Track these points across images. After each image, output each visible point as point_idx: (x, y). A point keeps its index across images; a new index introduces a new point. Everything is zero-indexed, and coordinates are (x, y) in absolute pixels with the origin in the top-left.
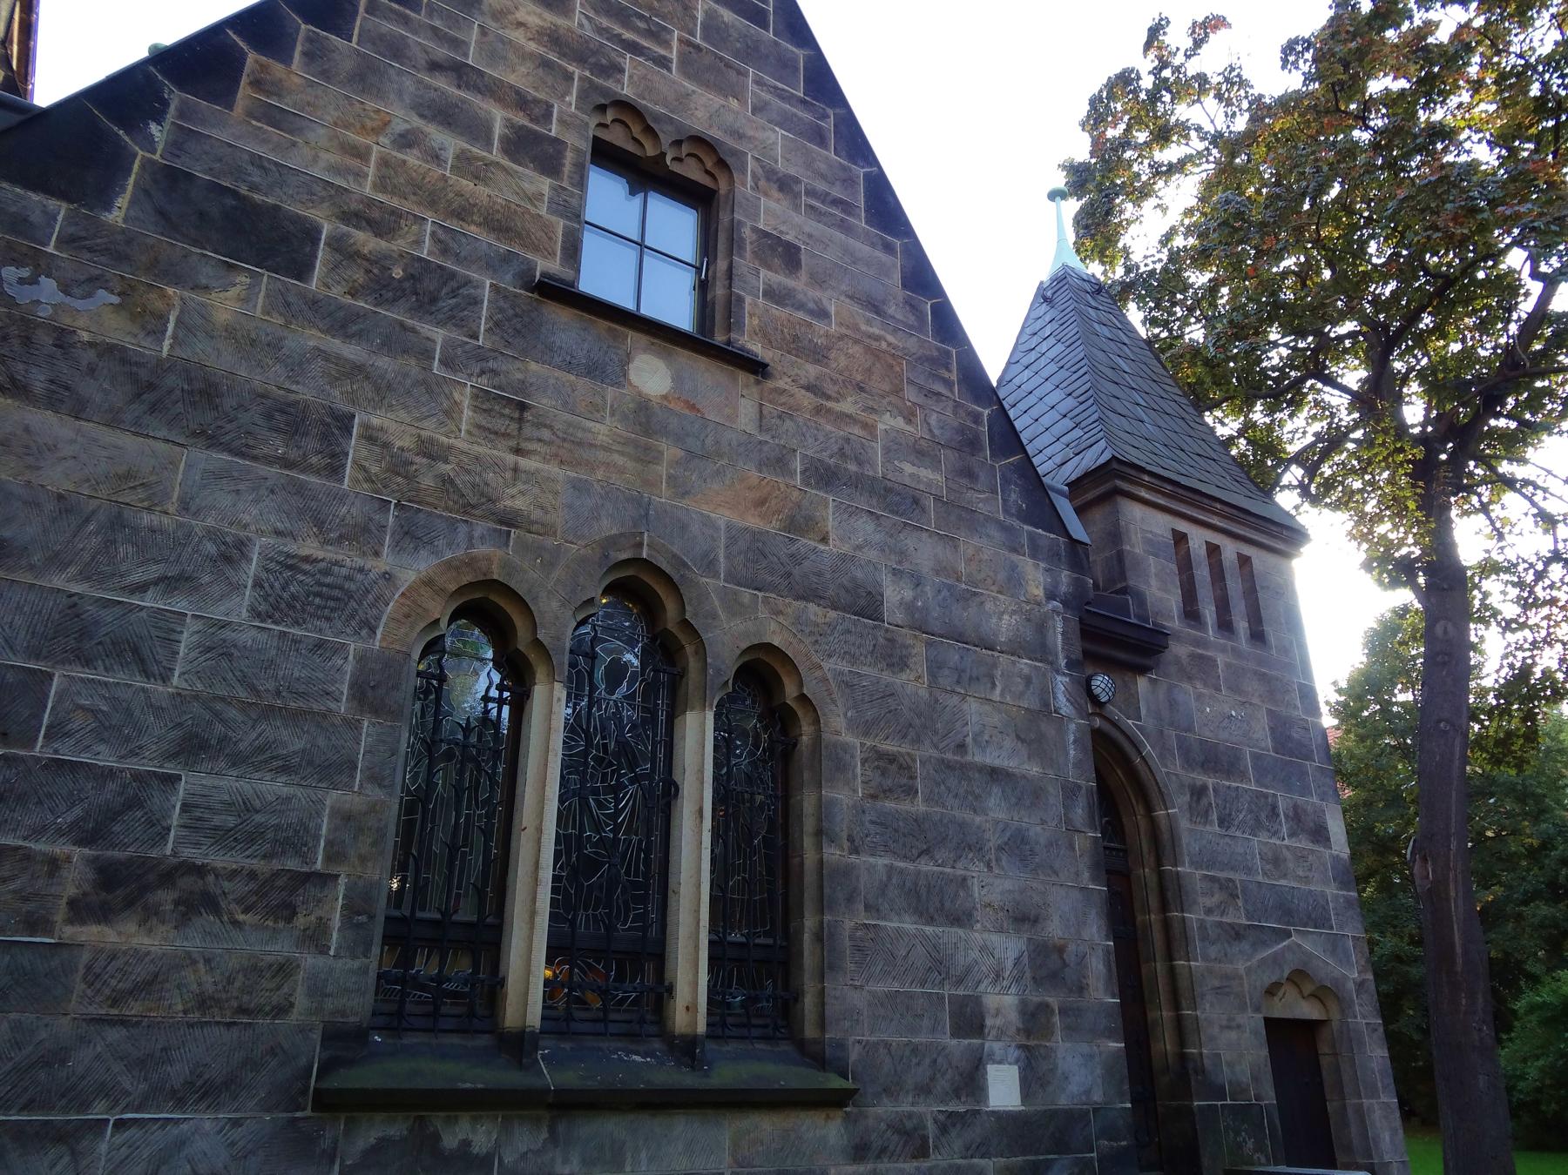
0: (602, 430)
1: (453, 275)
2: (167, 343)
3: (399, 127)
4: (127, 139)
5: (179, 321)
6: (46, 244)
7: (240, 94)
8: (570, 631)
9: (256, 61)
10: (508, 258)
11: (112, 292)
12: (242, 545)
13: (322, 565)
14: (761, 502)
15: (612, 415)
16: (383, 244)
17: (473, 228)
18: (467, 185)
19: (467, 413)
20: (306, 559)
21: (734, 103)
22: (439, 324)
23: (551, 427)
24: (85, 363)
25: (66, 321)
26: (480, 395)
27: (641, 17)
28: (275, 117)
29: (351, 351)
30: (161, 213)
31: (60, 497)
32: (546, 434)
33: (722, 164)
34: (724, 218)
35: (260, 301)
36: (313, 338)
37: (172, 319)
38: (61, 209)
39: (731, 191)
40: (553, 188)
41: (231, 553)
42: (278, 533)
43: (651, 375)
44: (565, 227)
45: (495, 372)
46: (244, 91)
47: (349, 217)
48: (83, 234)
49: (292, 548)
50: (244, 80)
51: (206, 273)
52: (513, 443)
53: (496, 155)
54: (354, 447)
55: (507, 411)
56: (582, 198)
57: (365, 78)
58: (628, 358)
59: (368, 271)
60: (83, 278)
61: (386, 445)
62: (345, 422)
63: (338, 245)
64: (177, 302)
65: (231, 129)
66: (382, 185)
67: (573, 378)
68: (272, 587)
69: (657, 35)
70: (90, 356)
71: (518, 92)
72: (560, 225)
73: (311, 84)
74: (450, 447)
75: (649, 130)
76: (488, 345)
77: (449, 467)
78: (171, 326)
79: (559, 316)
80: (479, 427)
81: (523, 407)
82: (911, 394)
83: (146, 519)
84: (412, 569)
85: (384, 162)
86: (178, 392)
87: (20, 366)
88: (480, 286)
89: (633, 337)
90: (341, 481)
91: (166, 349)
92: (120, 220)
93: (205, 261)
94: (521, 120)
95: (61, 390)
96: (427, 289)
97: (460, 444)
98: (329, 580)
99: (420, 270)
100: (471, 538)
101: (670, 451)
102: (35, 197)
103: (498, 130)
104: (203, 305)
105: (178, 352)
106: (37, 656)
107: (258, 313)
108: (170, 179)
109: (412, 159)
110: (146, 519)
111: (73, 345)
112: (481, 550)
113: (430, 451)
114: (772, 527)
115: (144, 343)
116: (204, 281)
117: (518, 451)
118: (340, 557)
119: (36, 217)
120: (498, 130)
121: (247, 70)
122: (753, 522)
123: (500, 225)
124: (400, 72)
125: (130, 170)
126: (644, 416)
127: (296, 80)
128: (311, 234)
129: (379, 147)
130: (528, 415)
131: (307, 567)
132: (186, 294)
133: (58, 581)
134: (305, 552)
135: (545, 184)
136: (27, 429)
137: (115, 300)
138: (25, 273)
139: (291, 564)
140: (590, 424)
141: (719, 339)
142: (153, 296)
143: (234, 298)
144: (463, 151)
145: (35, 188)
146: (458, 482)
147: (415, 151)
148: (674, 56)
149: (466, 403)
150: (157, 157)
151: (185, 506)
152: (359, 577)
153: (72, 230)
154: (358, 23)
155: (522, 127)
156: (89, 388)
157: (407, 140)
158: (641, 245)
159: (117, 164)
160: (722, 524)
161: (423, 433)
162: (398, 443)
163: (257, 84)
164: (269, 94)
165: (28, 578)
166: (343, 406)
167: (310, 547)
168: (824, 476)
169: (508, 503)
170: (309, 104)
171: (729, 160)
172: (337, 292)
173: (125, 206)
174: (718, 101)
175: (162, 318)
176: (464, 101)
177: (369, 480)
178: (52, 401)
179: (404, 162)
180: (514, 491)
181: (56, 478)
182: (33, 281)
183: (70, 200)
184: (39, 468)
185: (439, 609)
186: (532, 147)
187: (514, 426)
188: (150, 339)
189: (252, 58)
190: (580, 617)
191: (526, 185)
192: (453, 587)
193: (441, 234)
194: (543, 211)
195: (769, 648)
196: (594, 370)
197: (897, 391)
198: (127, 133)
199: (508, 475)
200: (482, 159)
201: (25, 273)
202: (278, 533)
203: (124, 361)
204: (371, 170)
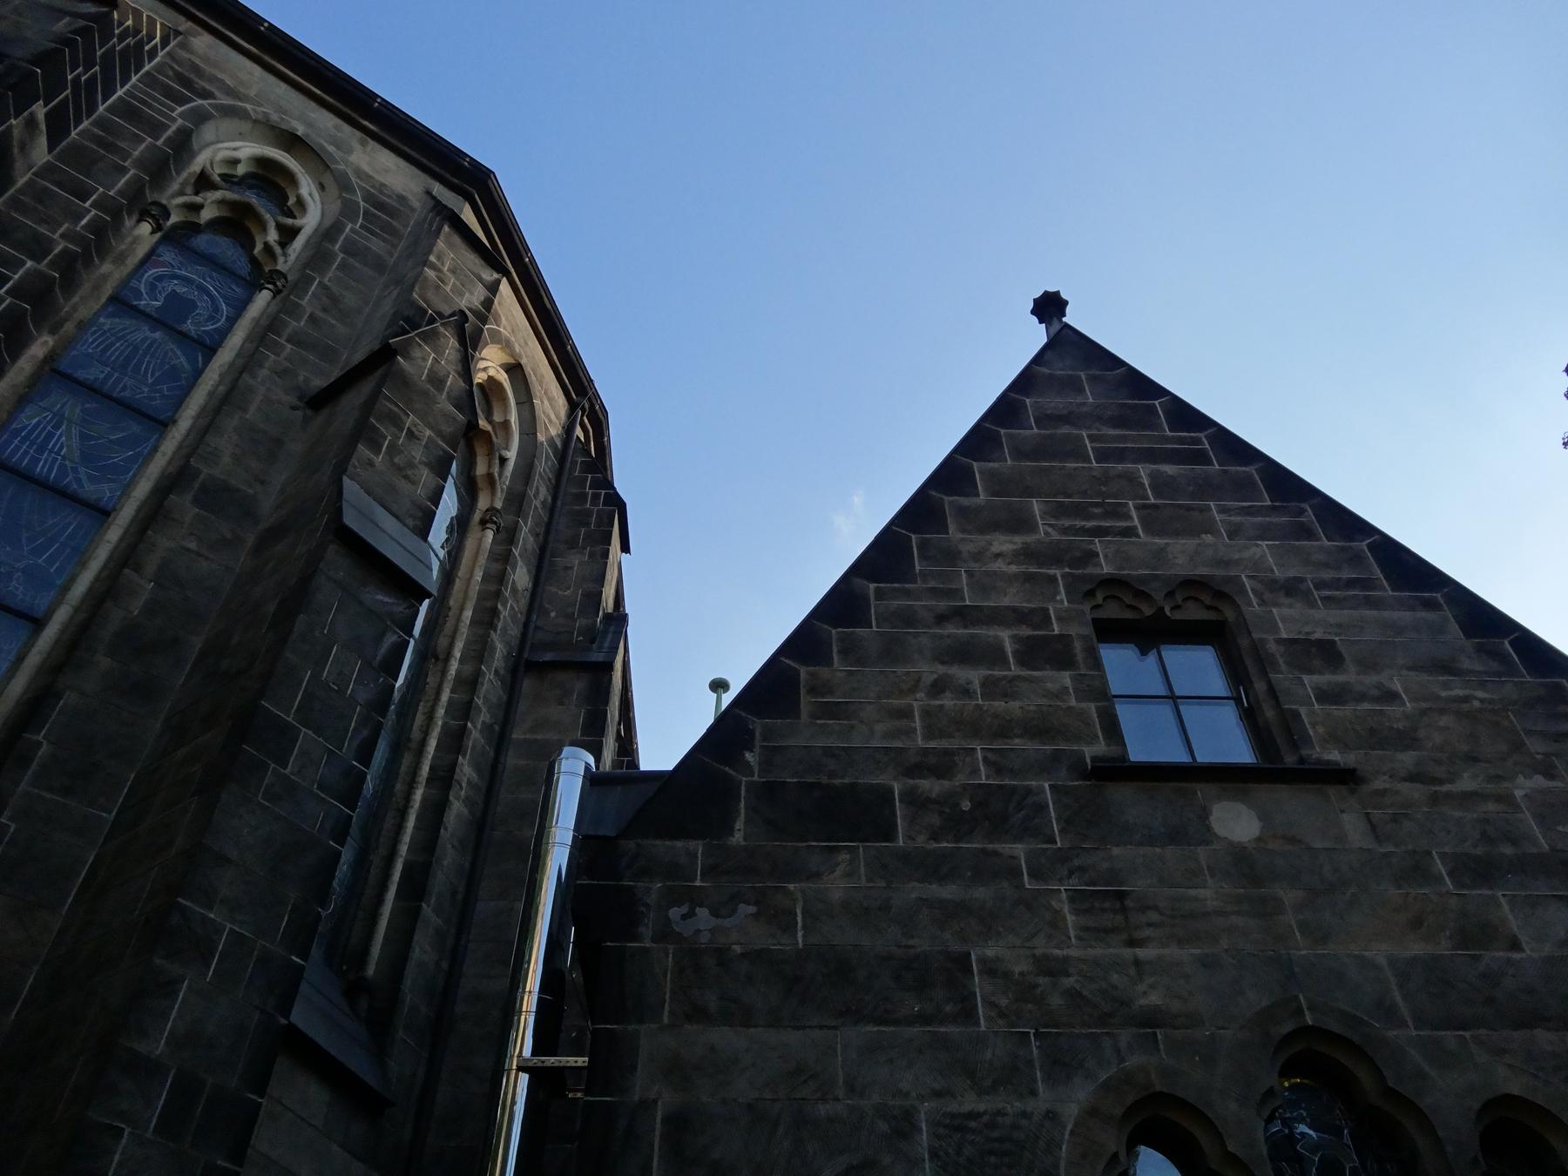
0: (1208, 894)
1: (1014, 789)
2: (800, 934)
3: (928, 679)
8: (1260, 1135)
10: (1056, 756)
12: (909, 1115)
13: (985, 1119)
14: (1417, 923)
15: (1213, 876)
16: (946, 783)
17: (1017, 741)
18: (999, 705)
19: (1070, 918)
20: (972, 1115)
21: (1208, 538)
22: (1017, 839)
23: (1156, 908)
26: (1075, 897)
27: (1096, 505)
28: (832, 711)
29: (949, 892)
32: (1154, 916)
33: (1220, 595)
34: (1244, 642)
35: (862, 870)
36: (914, 890)
38: (698, 846)
39: (1240, 613)
40: (1073, 679)
41: (904, 1126)
42: (938, 1094)
43: (1236, 822)
44: (1097, 708)
45: (1082, 869)
46: (806, 701)
47: (914, 770)
49: (953, 1107)
50: (803, 691)
52: (1124, 936)
53: (1015, 670)
54: (979, 985)
55: (1107, 905)
56: (1103, 677)
57: (892, 651)
58: (1204, 814)
59: (941, 813)
61: (1007, 975)
62: (963, 961)
63: (911, 798)
64: (799, 895)
65: (805, 734)
66: (930, 733)
67: (1158, 850)
68: (947, 1154)
69: (1117, 512)
71: (1014, 610)
72: (1092, 708)
74: (1066, 959)
75: (1142, 595)
76: (1067, 845)
77: (1072, 979)
78: (799, 919)
79: (1121, 794)
80: (1088, 929)
81: (1121, 896)
82: (1536, 746)
83: (823, 1110)
84: (1074, 1100)
85: (927, 713)
88: (1042, 790)
89: (1201, 790)
90: (978, 1024)
94: (1026, 631)
96: (998, 811)
97: (1073, 953)
98: (996, 1134)
99: (983, 796)
100: (1118, 1051)
101: (1289, 896)
102: (679, 844)
103: (1009, 648)
107: (863, 882)
108: (769, 791)
109: (948, 701)
110: (823, 1110)
112: (1134, 1061)
113: (1052, 968)
114: (1444, 948)
117: (1132, 943)
118: (1001, 1105)
120: (1009, 648)
122: (1417, 948)
123: (1039, 728)
124: (916, 635)
126: (1242, 863)
127: (839, 674)
128: (885, 795)
129: (918, 701)
130: (1129, 903)
131: (973, 1124)
134: (967, 1108)
135: (1066, 678)
137: (752, 909)
138: (684, 909)
139: (957, 1125)
140: (1193, 892)
141: (1290, 760)
143: (842, 876)
144: (987, 678)
146: (1085, 993)
147: (948, 694)
148: (1136, 522)
149: (1066, 909)
150: (756, 778)
151: (851, 1088)
152: (1024, 1122)
155: (1029, 637)
157: (938, 688)
158: (1173, 698)
160: (1382, 961)
161: (1038, 952)
162: (1017, 969)
163: (812, 690)
166: (956, 947)
167: (969, 1102)
168: (1478, 870)
169: (1143, 1002)
171: (1226, 589)
172: (921, 840)
174: (1190, 543)
176: (972, 636)
177: (1002, 1015)
179: (942, 706)
180: (1141, 988)
182: (690, 915)
185: (1112, 1141)
186: (1044, 652)
187: (1119, 918)
189: (804, 672)
190: (1266, 1114)
191: (1049, 685)
192: (1119, 1111)
193: (990, 755)
194: (1073, 703)
195: (1508, 1100)
196: (1176, 836)
197: (1518, 746)
199: (1132, 971)
200: (1005, 677)
201: (684, 909)
202: (938, 1094)
204: (918, 723)
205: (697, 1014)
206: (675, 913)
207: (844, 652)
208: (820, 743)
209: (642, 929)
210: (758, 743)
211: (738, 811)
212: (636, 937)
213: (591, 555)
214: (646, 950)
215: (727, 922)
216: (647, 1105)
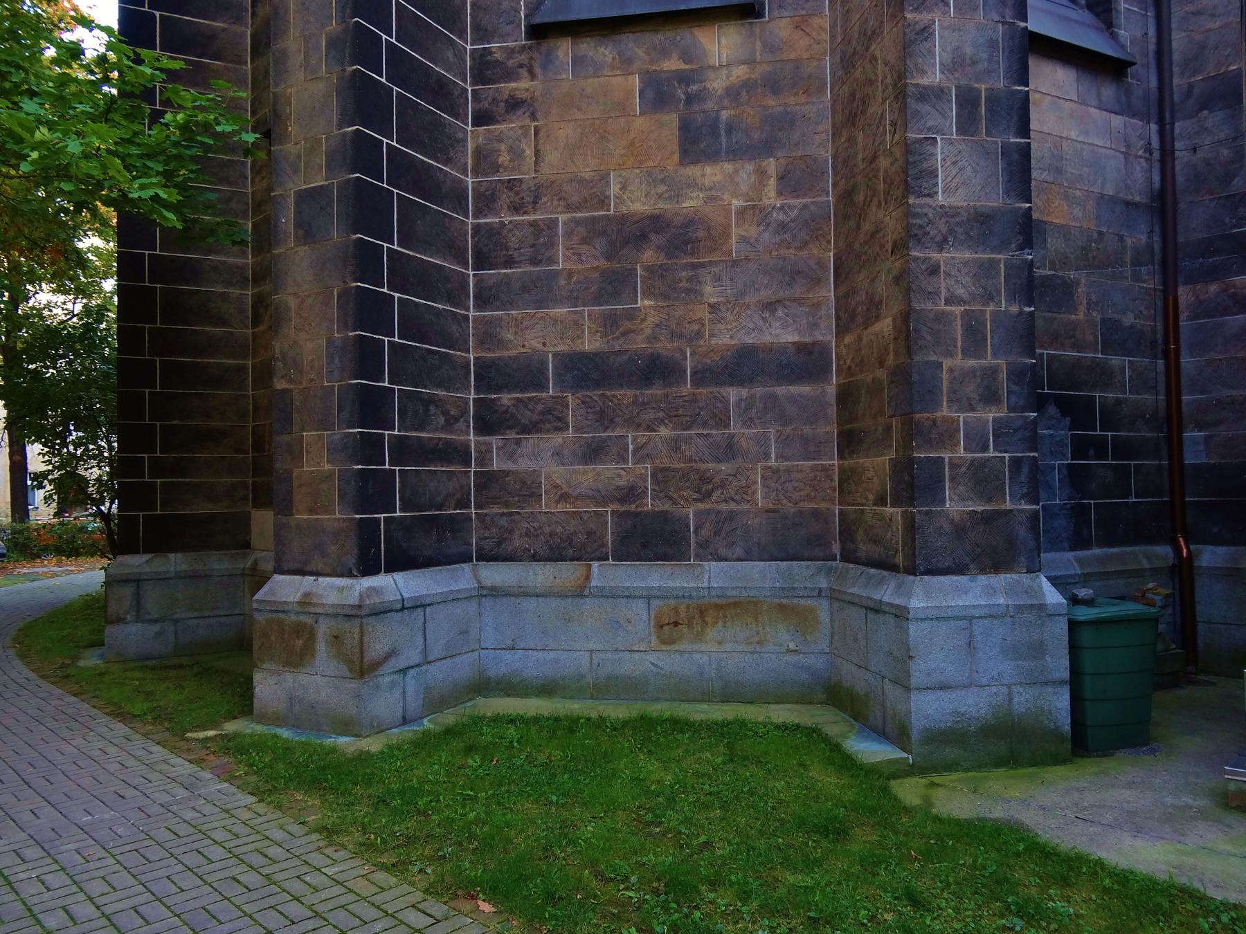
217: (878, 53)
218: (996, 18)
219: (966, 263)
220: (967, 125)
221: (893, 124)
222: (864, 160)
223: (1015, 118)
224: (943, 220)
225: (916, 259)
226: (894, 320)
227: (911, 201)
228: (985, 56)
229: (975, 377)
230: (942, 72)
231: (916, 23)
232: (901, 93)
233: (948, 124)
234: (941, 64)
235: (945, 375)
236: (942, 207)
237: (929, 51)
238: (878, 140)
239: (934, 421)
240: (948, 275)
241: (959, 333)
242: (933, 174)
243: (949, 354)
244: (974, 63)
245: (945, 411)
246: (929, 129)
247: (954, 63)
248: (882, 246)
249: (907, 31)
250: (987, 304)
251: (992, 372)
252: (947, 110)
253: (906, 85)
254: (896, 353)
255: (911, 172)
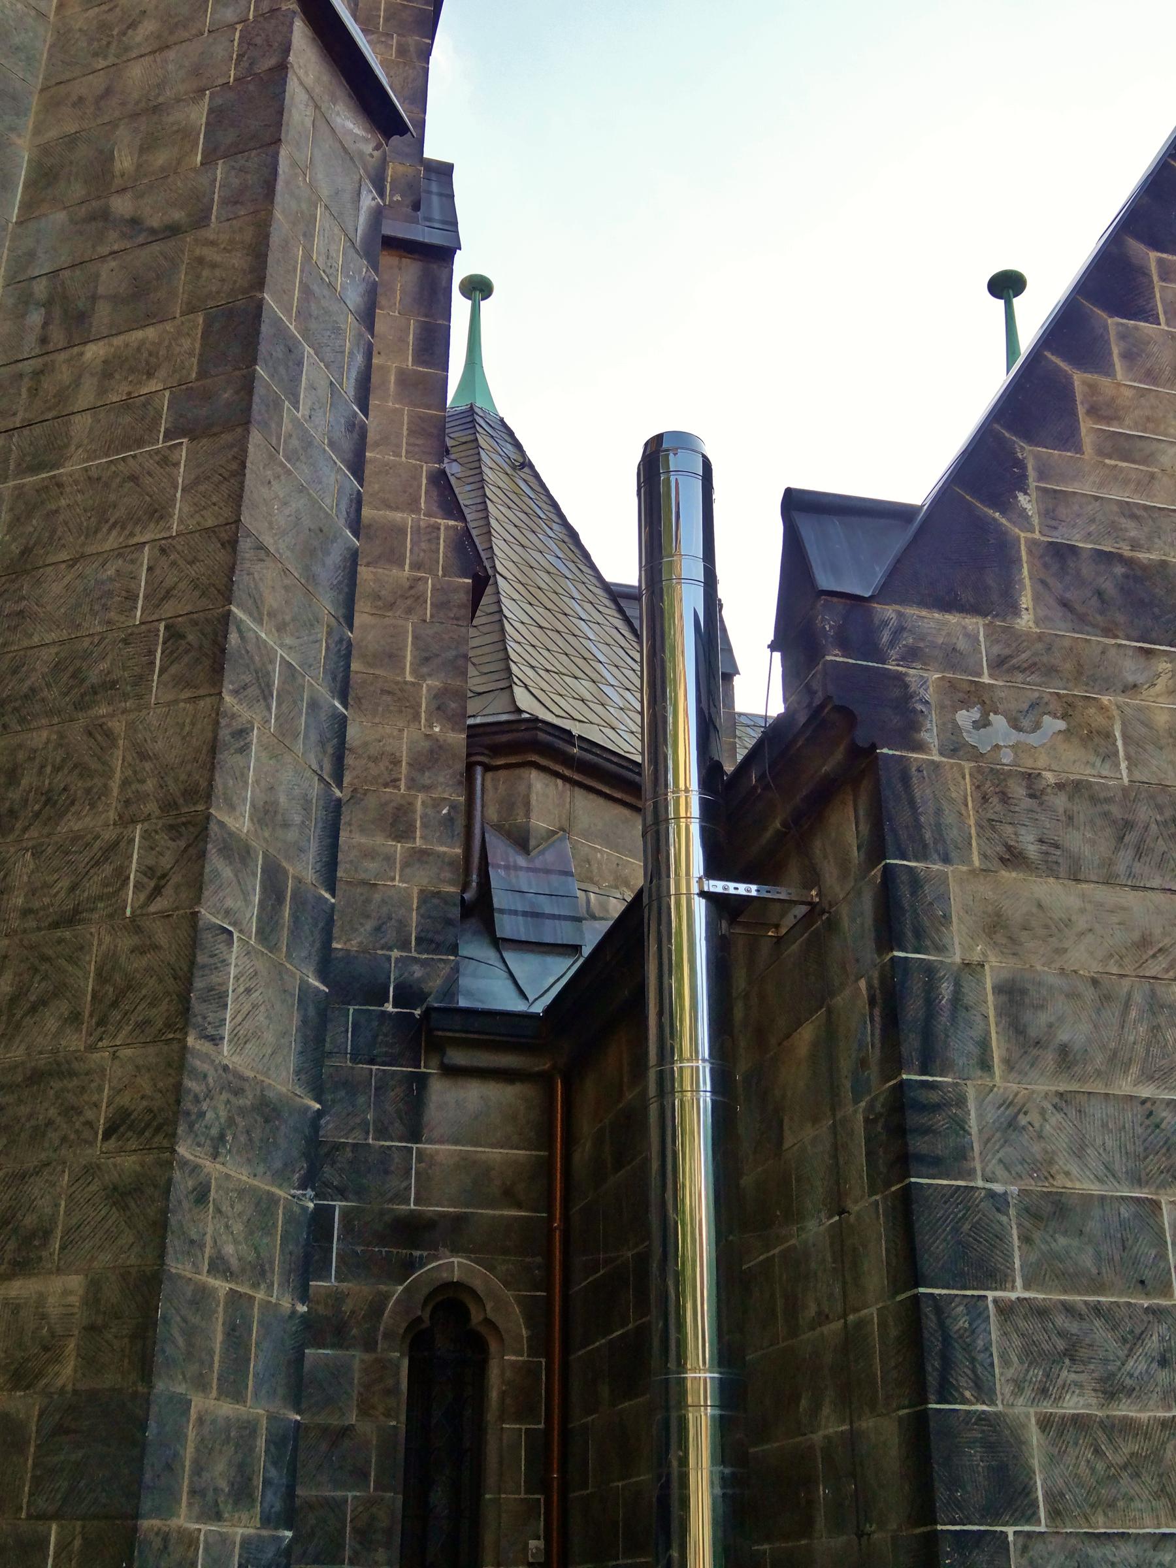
2: (1123, 765)
4: (1004, 521)
5: (1125, 737)
6: (980, 675)
7: (1083, 431)
9: (1084, 382)
11: (1055, 717)
24: (1061, 810)
25: (1028, 763)
30: (1065, 604)
31: (1095, 982)
37: (1118, 734)
38: (976, 624)
46: (1087, 427)
48: (1007, 652)
50: (1081, 410)
51: (1130, 669)
60: (1025, 706)
70: (1060, 801)
73: (1142, 393)
78: (1120, 743)
86: (1154, 826)
87: (1009, 829)
91: (1125, 773)
92: (1031, 624)
93: (1120, 653)
95: (1052, 850)
102: (953, 619)
104: (1140, 709)
105: (1138, 776)
106: (1138, 1180)
111: (1043, 792)
115: (1104, 773)
116: (1131, 679)
119: (962, 644)
121: (1079, 398)
125: (1020, 559)
132: (1121, 699)
133: (1125, 1086)
136: (1040, 906)
137: (1061, 725)
138: (975, 714)
142: (1092, 711)
145: (947, 606)
150: (1037, 536)
153: (996, 650)
154: (1158, 296)
156: (1076, 840)
159: (1003, 554)
163: (1093, 411)
164: (1109, 420)
165: (1099, 1087)
170: (1148, 419)
173: (1031, 606)
175: (1108, 735)
178: (1050, 868)
181: (1083, 957)
182: (982, 723)
183: (985, 615)
184: (1065, 950)
188: (1107, 765)
189: (1079, 379)
198: (1003, 513)
201: (975, 714)
203: (1094, 800)
205: (1013, 858)
206: (965, 718)
207: (1128, 356)
208: (1116, 494)
209: (924, 736)
210: (1032, 482)
211: (1021, 581)
212: (920, 747)
213: (402, 51)
214: (936, 766)
215: (1032, 739)
216: (972, 968)
217: (118, 726)
218: (315, 767)
219: (242, 1192)
220: (267, 930)
221: (148, 871)
222: (26, 912)
223: (318, 945)
224: (225, 1096)
225: (184, 1163)
226: (94, 1286)
227: (190, 1040)
228: (298, 819)
229: (228, 1440)
230: (251, 819)
231: (233, 716)
232: (188, 822)
233: (248, 916)
234: (253, 806)
235: (191, 1433)
236: (225, 1068)
237: (242, 775)
238: (92, 887)
239: (166, 1538)
240: (218, 1211)
241: (219, 1337)
242: (220, 1000)
243: (201, 1384)
244: (286, 825)
245: (183, 1520)
246: (228, 912)
247: (266, 812)
248: (70, 1111)
249: (223, 722)
250: (256, 1286)
251: (249, 1428)
252: (250, 888)
253: (208, 817)
254: (90, 1362)
255: (199, 984)
